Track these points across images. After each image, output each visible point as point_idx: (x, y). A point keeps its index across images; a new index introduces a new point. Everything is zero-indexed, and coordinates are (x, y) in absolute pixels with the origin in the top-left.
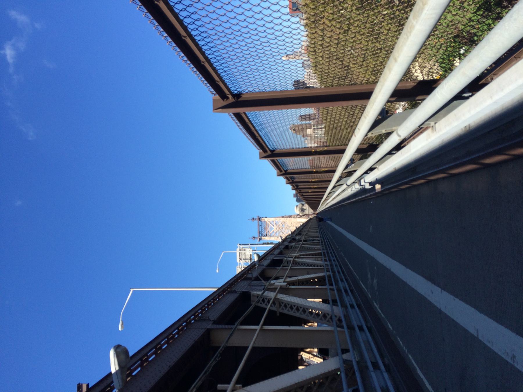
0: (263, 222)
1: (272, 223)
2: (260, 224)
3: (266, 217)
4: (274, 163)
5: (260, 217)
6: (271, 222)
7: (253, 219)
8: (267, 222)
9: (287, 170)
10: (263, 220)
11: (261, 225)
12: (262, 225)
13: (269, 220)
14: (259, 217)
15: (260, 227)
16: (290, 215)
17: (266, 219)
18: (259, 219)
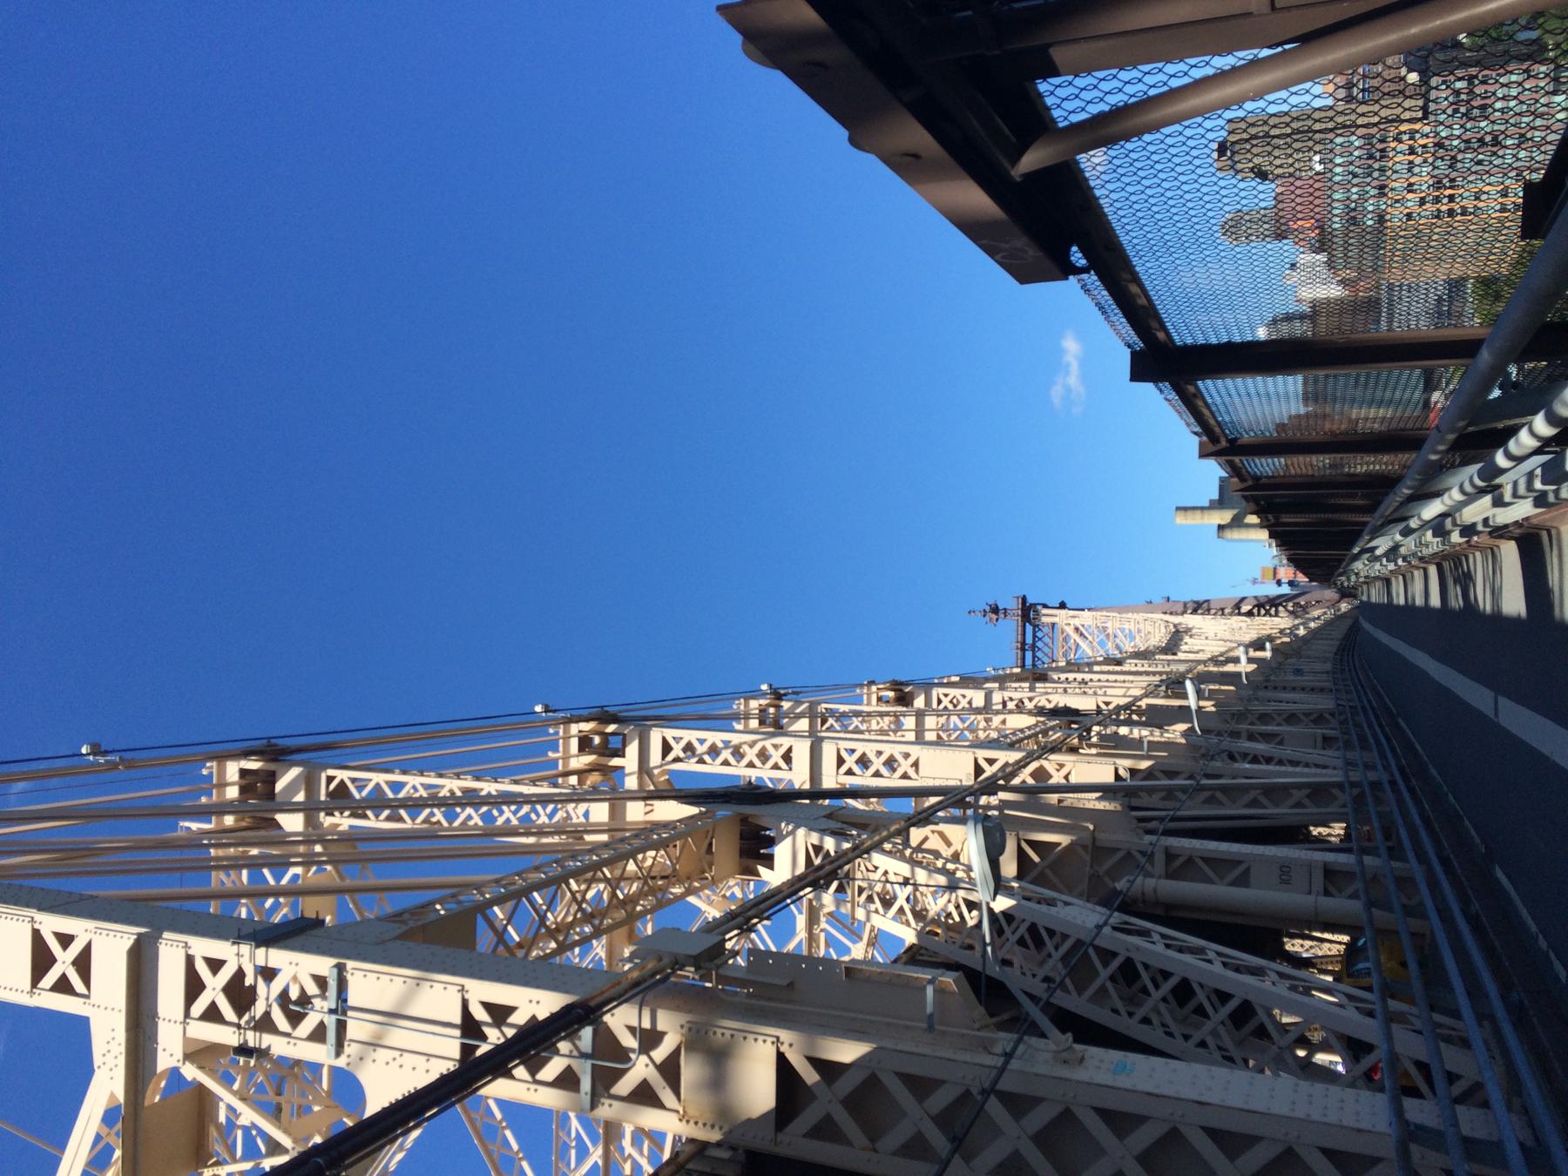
0: (1045, 630)
1: (1090, 638)
2: (1029, 640)
3: (1063, 606)
4: (1193, 405)
5: (1030, 600)
6: (1081, 628)
7: (995, 610)
8: (1066, 628)
9: (1235, 440)
10: (1048, 617)
11: (1033, 646)
12: (1039, 644)
13: (1077, 622)
14: (1024, 599)
15: (1029, 655)
16: (1201, 598)
17: (1061, 617)
18: (1028, 612)
